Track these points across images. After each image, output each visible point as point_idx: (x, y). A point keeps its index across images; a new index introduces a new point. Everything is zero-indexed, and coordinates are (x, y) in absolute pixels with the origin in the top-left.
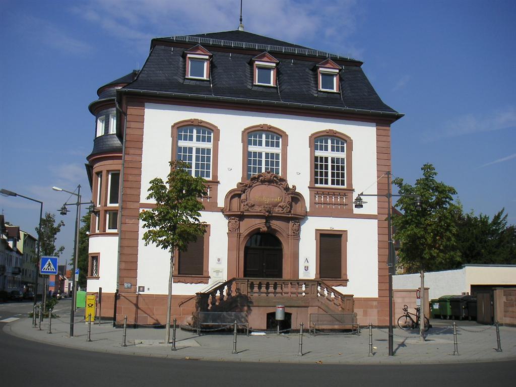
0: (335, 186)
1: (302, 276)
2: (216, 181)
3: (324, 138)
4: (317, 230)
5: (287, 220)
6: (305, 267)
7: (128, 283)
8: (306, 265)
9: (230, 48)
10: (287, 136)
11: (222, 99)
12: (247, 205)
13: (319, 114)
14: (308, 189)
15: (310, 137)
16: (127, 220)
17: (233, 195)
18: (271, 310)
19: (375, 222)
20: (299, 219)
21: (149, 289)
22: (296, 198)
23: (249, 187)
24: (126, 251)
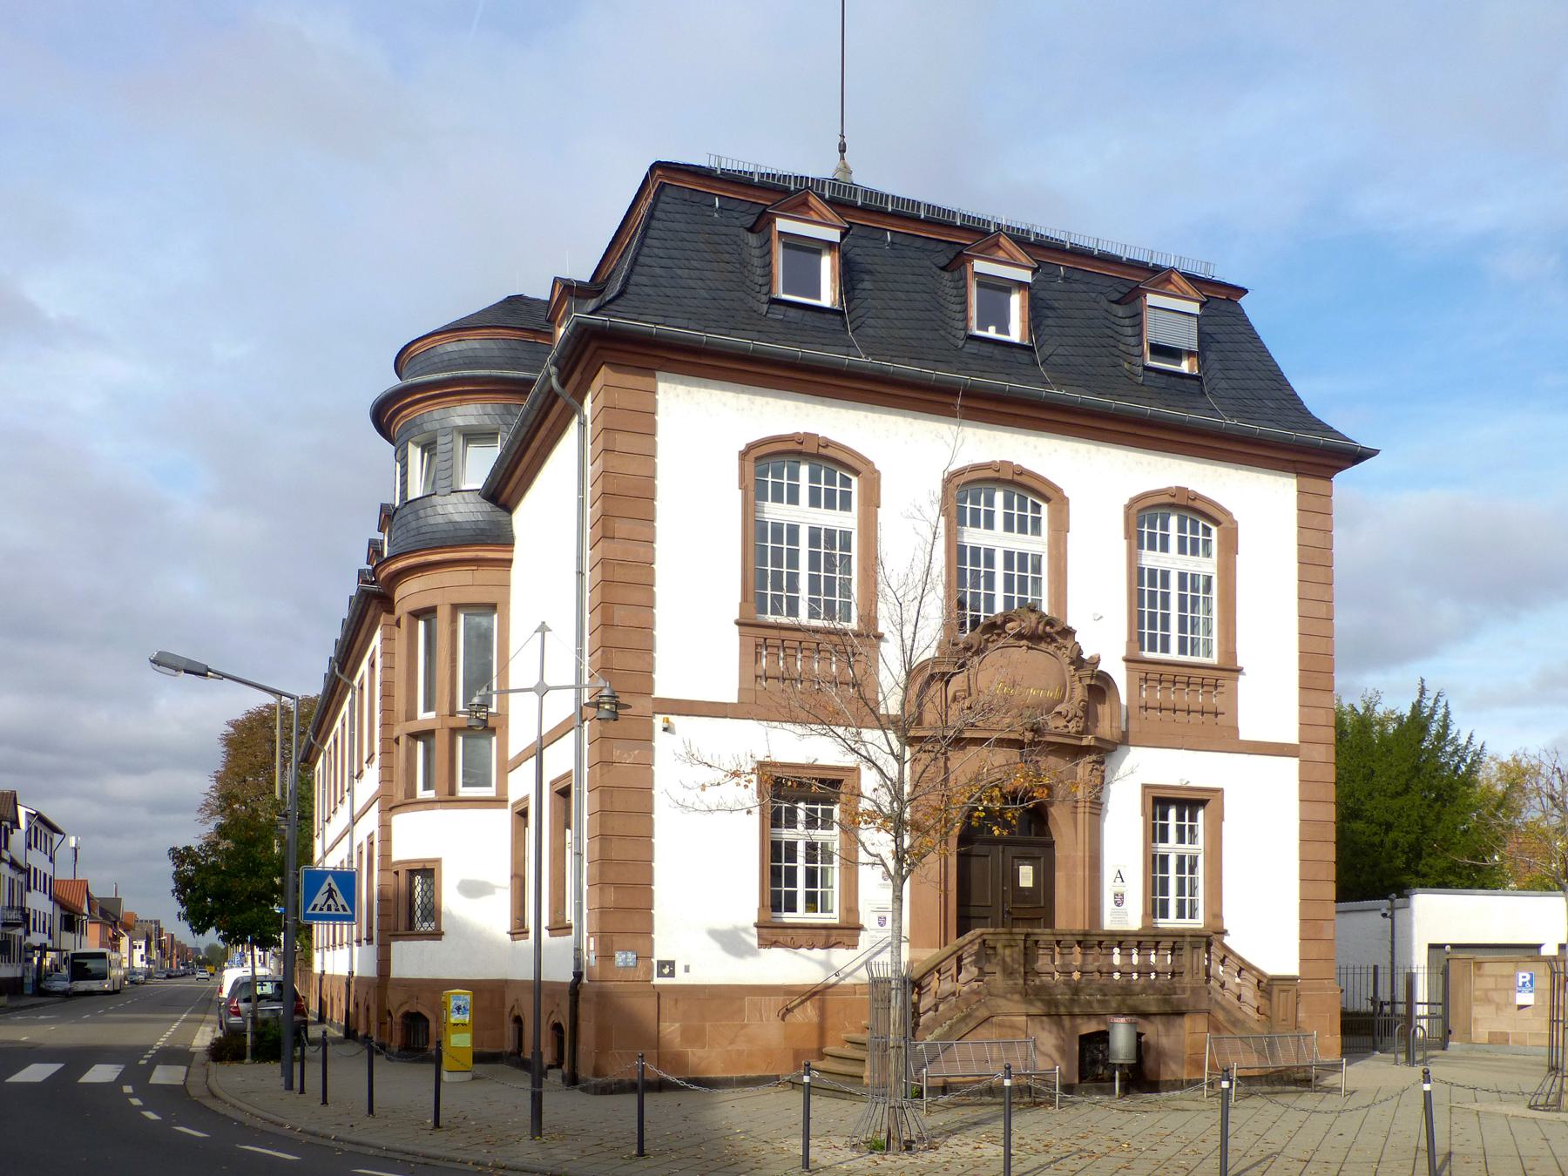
0: (1187, 658)
1: (1112, 920)
2: (1234, 667)
3: (1159, 511)
4: (1145, 787)
5: (1077, 752)
6: (1116, 895)
7: (624, 950)
8: (1118, 890)
9: (951, 226)
10: (1064, 501)
11: (1323, 445)
12: (970, 708)
13: (1134, 435)
14: (1123, 664)
15: (1128, 508)
16: (617, 753)
17: (924, 678)
18: (1090, 1027)
19: (1289, 768)
20: (1104, 752)
21: (687, 969)
22: (1101, 687)
23: (977, 653)
24: (618, 850)
